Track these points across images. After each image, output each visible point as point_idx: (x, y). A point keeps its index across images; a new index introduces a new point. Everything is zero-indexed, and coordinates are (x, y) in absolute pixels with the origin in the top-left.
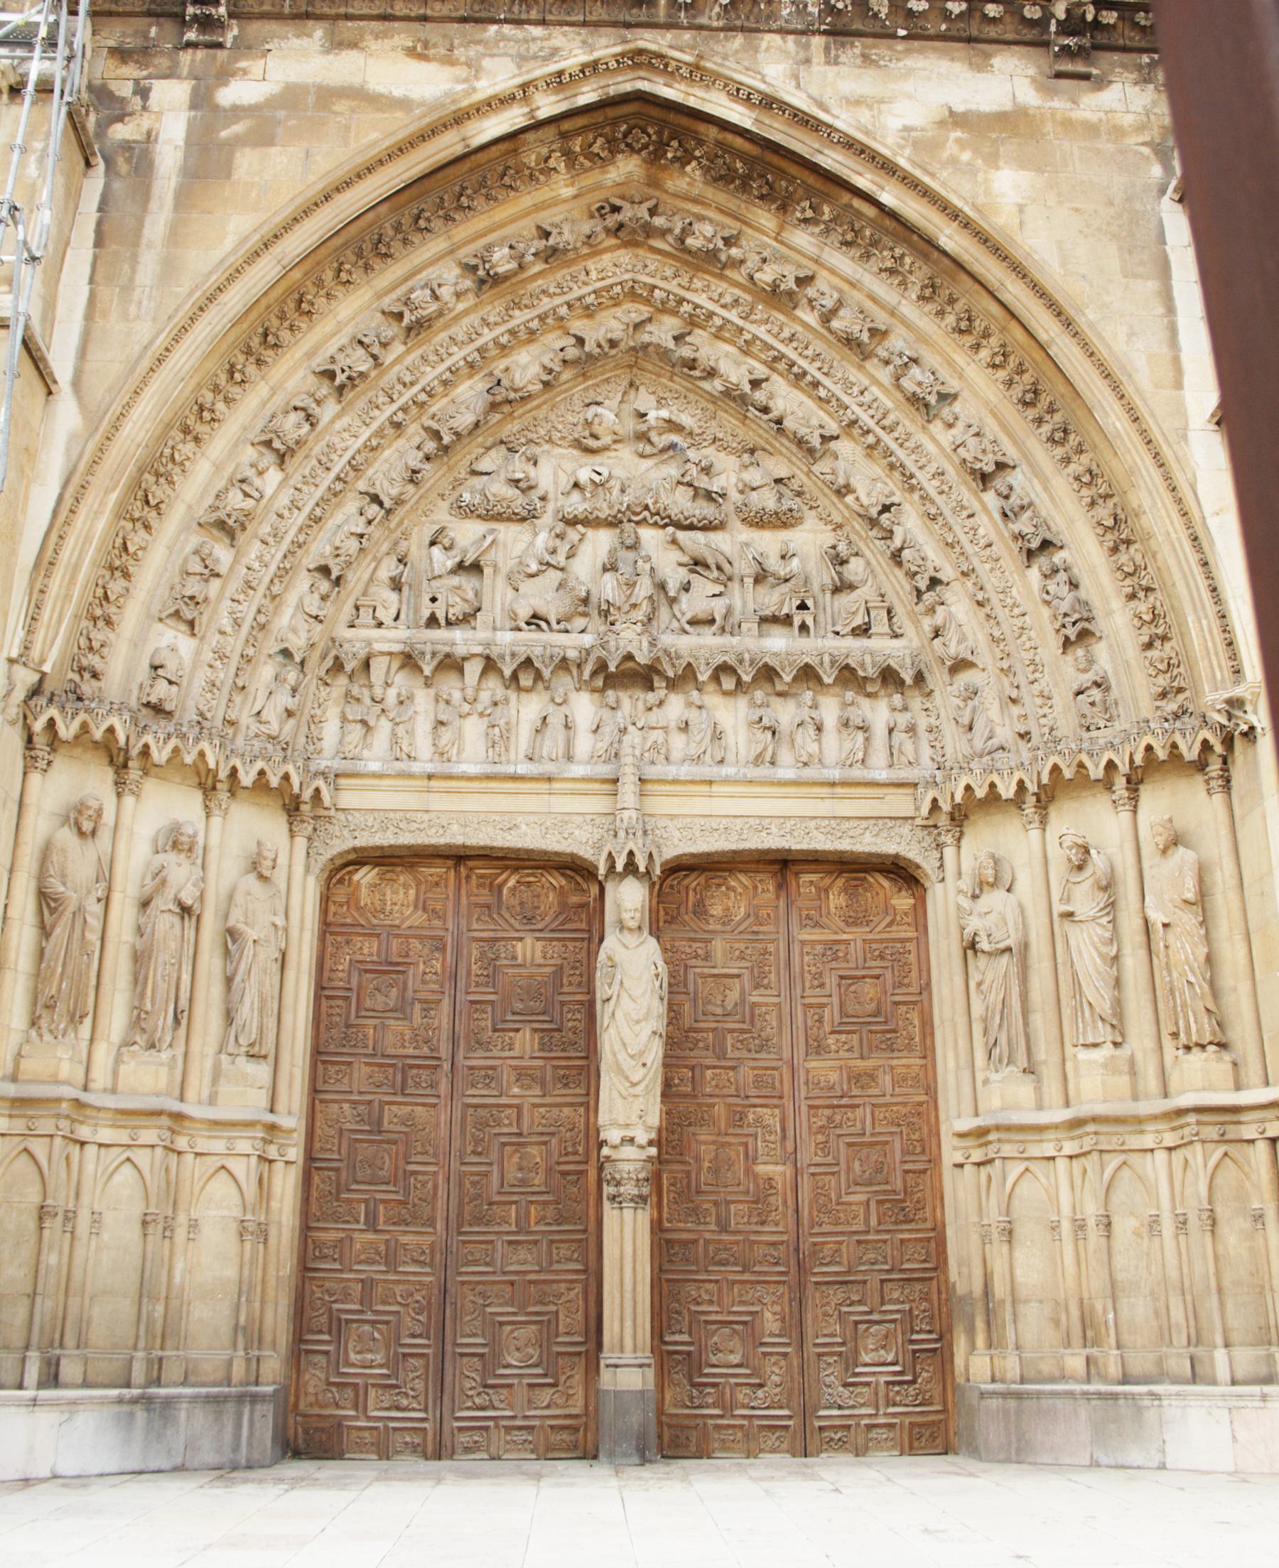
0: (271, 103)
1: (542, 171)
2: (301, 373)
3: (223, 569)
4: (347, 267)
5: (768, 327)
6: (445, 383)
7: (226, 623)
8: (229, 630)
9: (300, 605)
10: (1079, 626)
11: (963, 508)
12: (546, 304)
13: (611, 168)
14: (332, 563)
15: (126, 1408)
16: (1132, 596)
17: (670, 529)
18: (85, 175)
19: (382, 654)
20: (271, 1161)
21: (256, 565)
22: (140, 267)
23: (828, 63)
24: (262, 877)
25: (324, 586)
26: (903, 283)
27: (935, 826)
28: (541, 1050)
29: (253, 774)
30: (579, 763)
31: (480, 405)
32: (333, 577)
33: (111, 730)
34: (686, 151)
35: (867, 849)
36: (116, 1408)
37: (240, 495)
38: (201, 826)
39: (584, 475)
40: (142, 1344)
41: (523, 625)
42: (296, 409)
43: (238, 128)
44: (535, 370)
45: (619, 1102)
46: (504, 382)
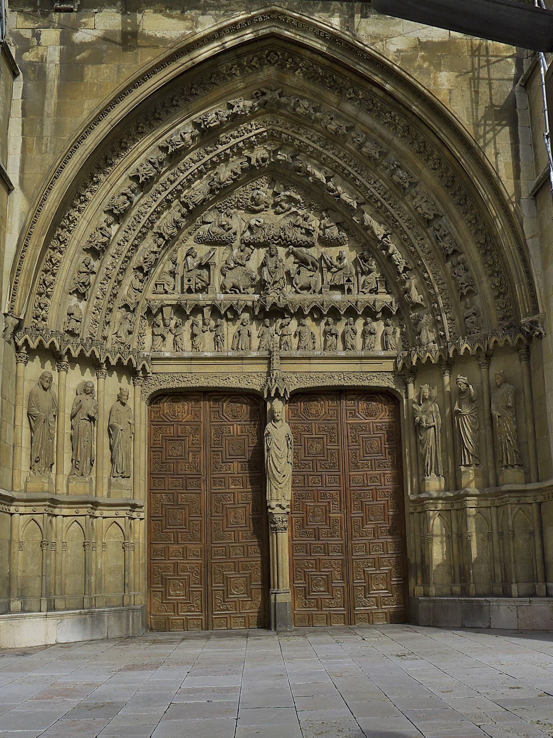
1: (229, 75)
4: (141, 125)
5: (333, 151)
6: (189, 181)
8: (100, 297)
10: (468, 288)
11: (419, 235)
12: (233, 142)
13: (261, 73)
14: (144, 265)
15: (83, 617)
16: (491, 275)
17: (291, 247)
18: (14, 79)
19: (168, 305)
20: (134, 519)
21: (110, 267)
22: (45, 127)
24: (124, 404)
25: (141, 275)
26: (395, 129)
27: (404, 375)
28: (242, 470)
30: (254, 351)
31: (206, 191)
34: (295, 63)
35: (375, 385)
36: (79, 617)
38: (95, 383)
39: (253, 222)
40: (87, 592)
41: (228, 291)
42: (123, 194)
44: (228, 174)
45: (275, 490)
46: (215, 179)
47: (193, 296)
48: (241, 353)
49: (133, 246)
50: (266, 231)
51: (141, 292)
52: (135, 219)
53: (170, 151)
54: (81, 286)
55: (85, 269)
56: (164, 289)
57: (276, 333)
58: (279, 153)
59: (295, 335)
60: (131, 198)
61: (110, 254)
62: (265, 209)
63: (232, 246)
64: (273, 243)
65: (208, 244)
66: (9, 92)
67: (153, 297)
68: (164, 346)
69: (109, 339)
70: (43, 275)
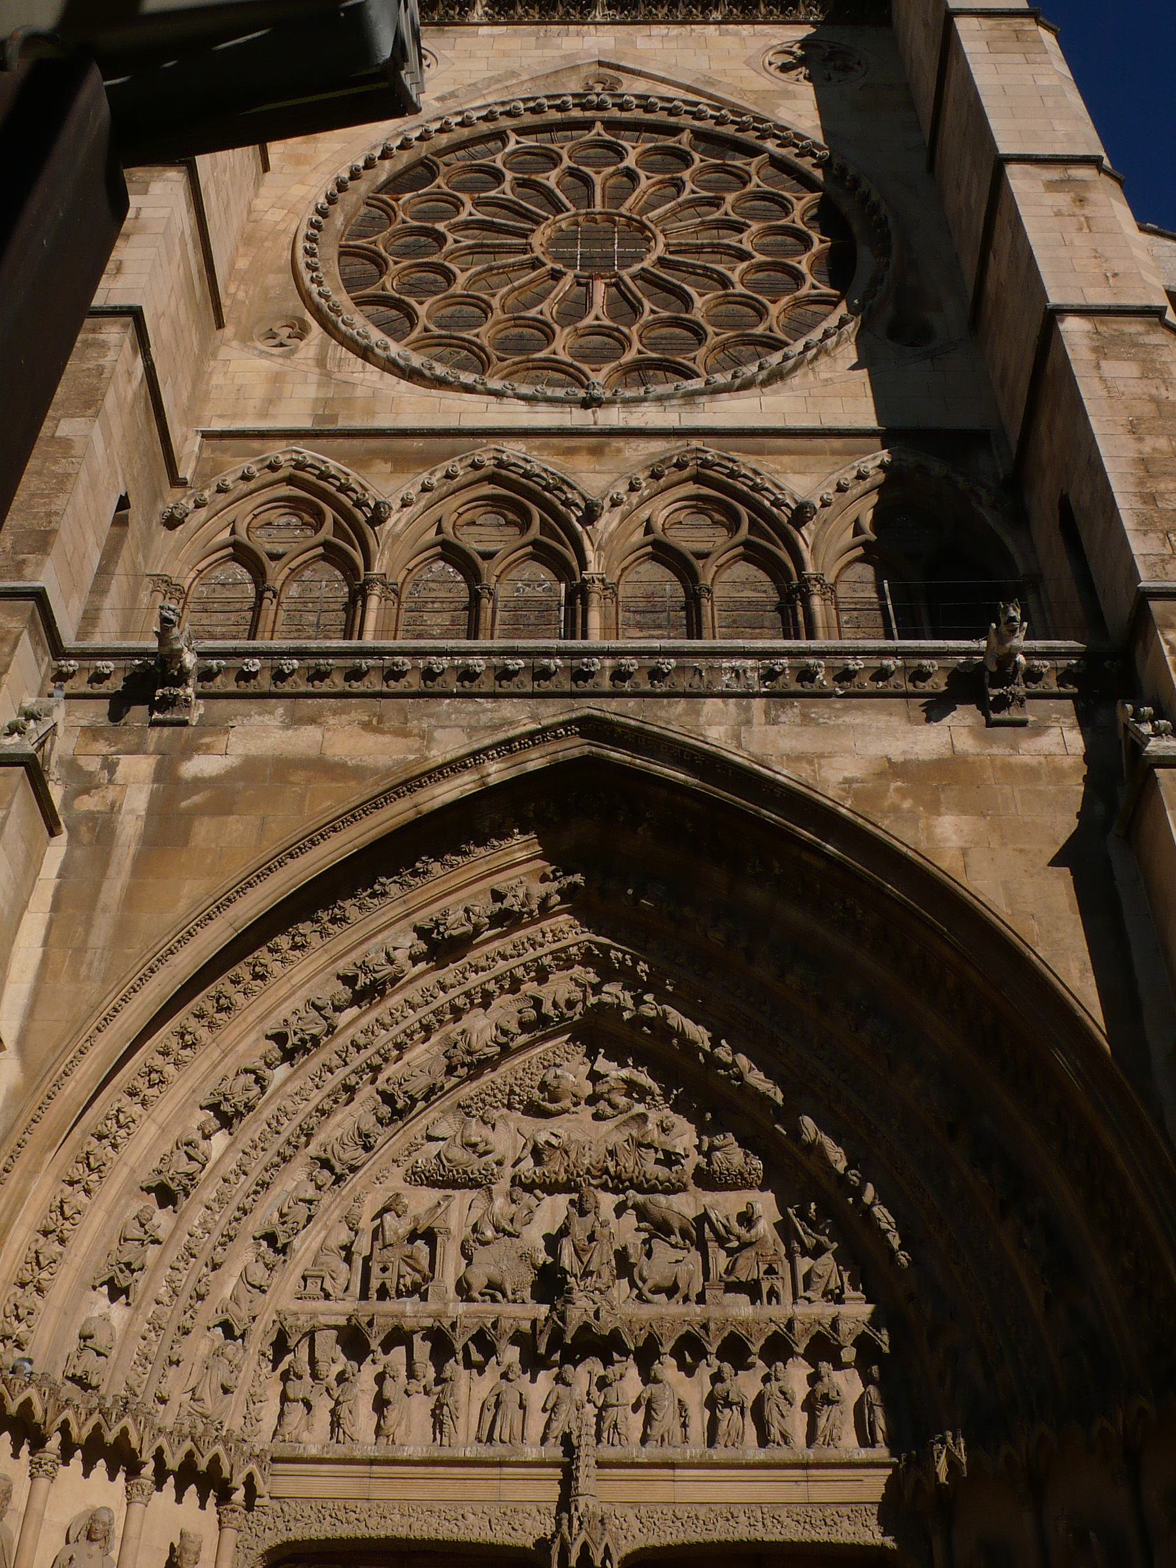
0: (231, 775)
2: (253, 1036)
3: (161, 1234)
7: (163, 1291)
8: (166, 1300)
9: (244, 1275)
14: (279, 1230)
17: (631, 1193)
19: (329, 1327)
21: (199, 1232)
23: (768, 723)
29: (180, 1456)
32: (279, 1245)
33: (28, 1403)
37: (185, 1158)
39: (542, 1138)
42: (247, 1071)
43: (197, 799)
46: (461, 1045)
47: (389, 1306)
48: (496, 1451)
49: (257, 1185)
50: (573, 1156)
51: (264, 1292)
52: (269, 1125)
53: (359, 984)
54: (122, 1271)
55: (137, 1233)
56: (322, 1289)
57: (589, 1401)
58: (604, 989)
59: (635, 1408)
60: (264, 1080)
61: (201, 1202)
62: (573, 1109)
63: (490, 1190)
64: (590, 1184)
65: (433, 1184)
66: (32, 863)
67: (296, 1306)
68: (309, 1427)
69: (173, 1405)
70: (37, 1241)
